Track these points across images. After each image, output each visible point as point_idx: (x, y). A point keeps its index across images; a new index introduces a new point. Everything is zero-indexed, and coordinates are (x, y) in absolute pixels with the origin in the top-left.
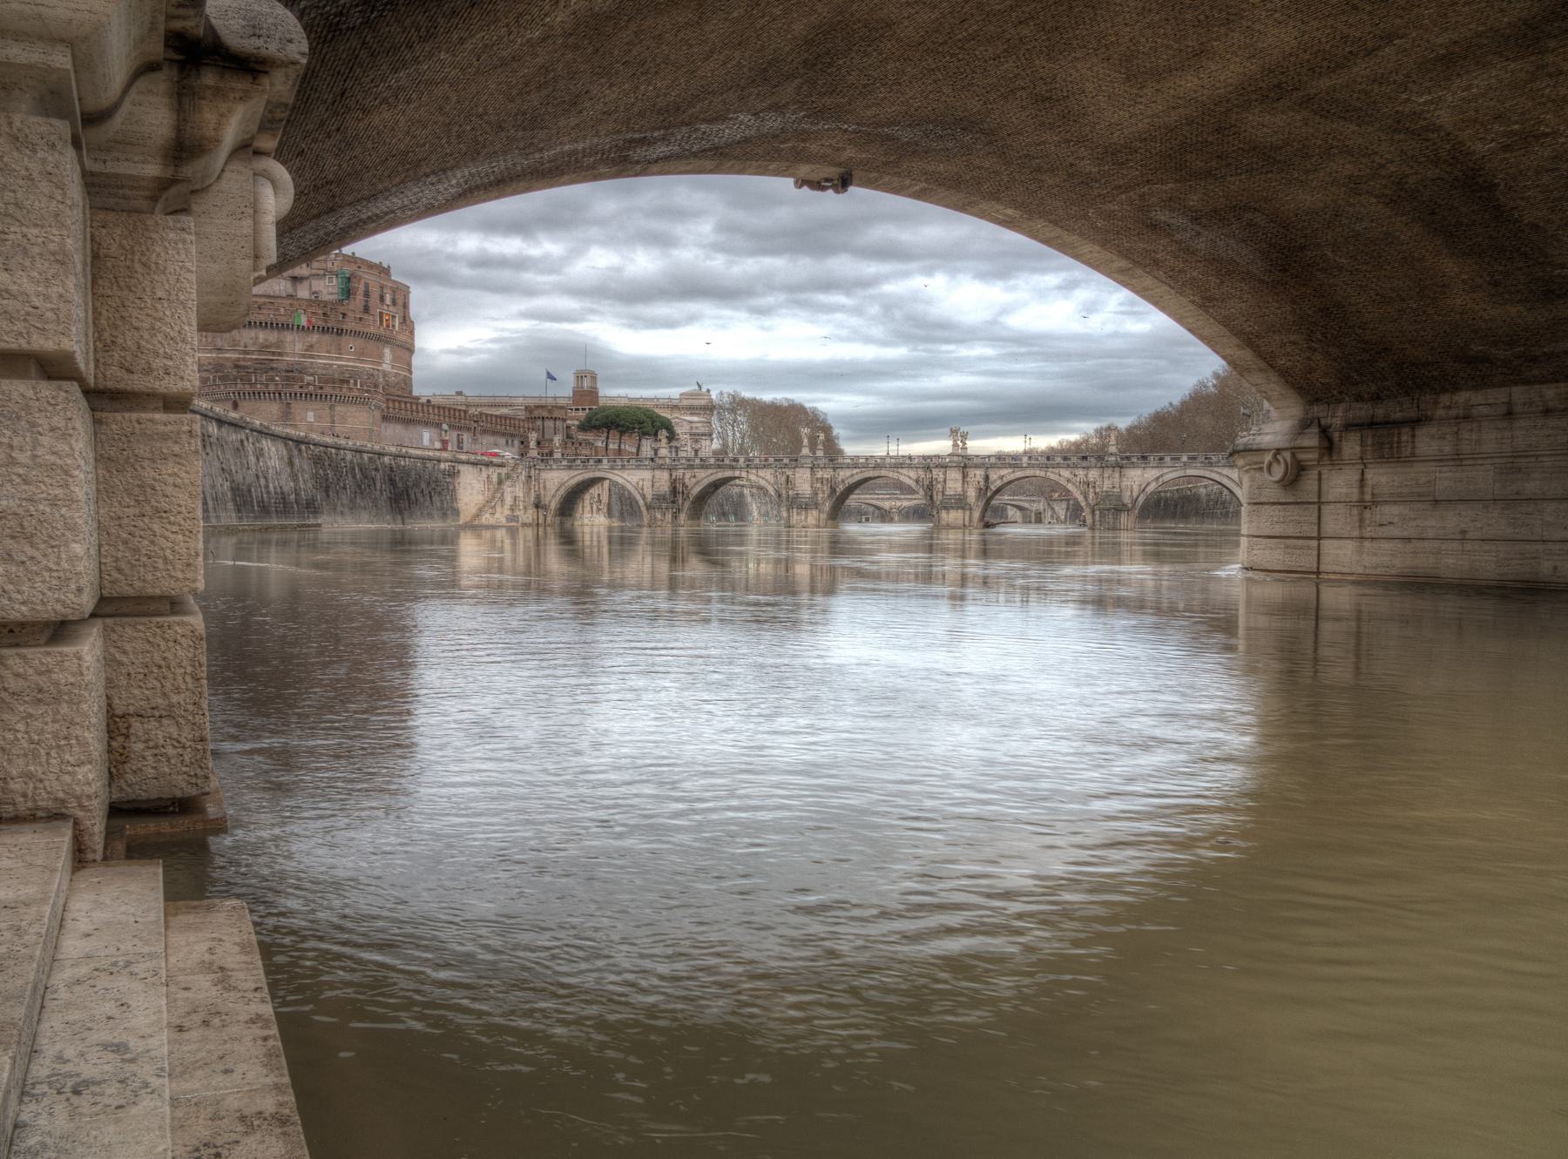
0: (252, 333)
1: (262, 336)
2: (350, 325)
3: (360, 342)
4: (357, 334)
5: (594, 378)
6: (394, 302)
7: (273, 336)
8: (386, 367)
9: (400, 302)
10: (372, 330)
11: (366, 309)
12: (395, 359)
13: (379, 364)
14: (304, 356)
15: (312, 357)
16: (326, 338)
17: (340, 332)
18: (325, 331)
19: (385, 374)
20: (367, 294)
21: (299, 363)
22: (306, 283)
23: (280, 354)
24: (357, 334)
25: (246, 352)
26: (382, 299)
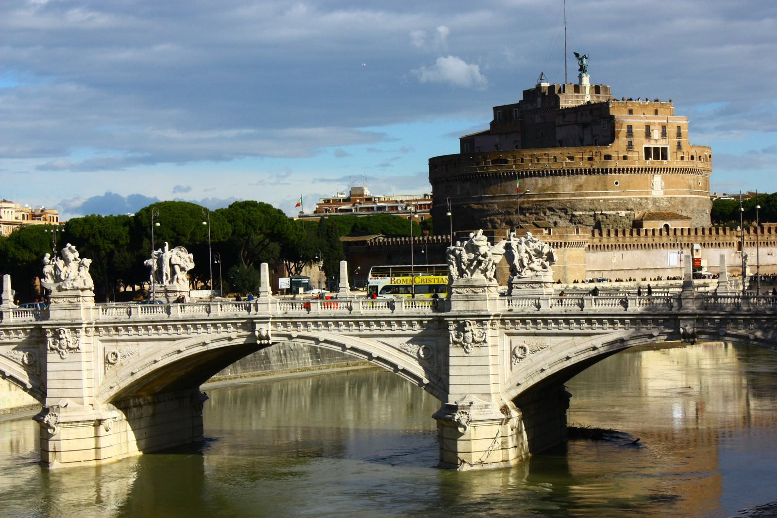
1: (540, 181)
2: (611, 165)
6: (664, 134)
7: (549, 181)
10: (636, 165)
11: (630, 146)
12: (668, 185)
14: (574, 195)
15: (582, 195)
16: (594, 177)
17: (605, 171)
18: (591, 172)
19: (655, 201)
21: (570, 201)
23: (555, 195)
26: (648, 134)
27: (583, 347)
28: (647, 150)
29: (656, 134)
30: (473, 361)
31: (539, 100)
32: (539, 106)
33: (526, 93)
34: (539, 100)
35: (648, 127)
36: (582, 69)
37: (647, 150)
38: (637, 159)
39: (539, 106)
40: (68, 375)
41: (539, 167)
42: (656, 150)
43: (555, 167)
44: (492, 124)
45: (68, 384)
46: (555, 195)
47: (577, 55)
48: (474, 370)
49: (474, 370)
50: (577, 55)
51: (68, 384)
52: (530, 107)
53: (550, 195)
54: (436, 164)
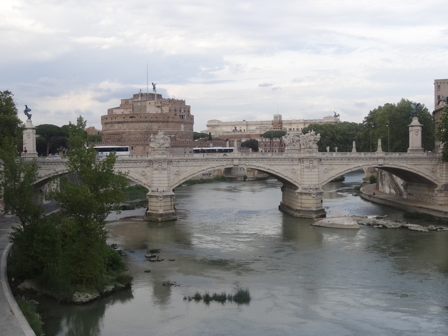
0: (144, 124)
1: (147, 124)
2: (170, 120)
3: (173, 124)
4: (172, 122)
5: (280, 116)
6: (185, 111)
7: (150, 124)
8: (182, 130)
9: (187, 111)
10: (177, 120)
11: (175, 115)
13: (180, 129)
16: (164, 123)
17: (168, 122)
18: (163, 122)
19: (182, 132)
20: (175, 110)
22: (160, 108)
23: (151, 129)
24: (172, 122)
25: (143, 129)
26: (180, 111)
27: (347, 169)
28: (180, 115)
29: (182, 111)
30: (312, 173)
31: (140, 98)
32: (140, 100)
33: (135, 96)
34: (140, 98)
35: (180, 108)
36: (154, 88)
37: (180, 115)
38: (178, 118)
39: (140, 100)
40: (161, 179)
41: (146, 120)
42: (182, 115)
43: (152, 120)
44: (120, 105)
45: (162, 182)
46: (151, 129)
47: (153, 84)
48: (312, 177)
49: (312, 177)
50: (153, 84)
51: (162, 182)
52: (136, 100)
53: (150, 129)
54: (104, 118)
